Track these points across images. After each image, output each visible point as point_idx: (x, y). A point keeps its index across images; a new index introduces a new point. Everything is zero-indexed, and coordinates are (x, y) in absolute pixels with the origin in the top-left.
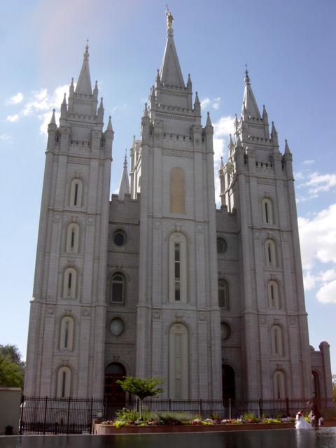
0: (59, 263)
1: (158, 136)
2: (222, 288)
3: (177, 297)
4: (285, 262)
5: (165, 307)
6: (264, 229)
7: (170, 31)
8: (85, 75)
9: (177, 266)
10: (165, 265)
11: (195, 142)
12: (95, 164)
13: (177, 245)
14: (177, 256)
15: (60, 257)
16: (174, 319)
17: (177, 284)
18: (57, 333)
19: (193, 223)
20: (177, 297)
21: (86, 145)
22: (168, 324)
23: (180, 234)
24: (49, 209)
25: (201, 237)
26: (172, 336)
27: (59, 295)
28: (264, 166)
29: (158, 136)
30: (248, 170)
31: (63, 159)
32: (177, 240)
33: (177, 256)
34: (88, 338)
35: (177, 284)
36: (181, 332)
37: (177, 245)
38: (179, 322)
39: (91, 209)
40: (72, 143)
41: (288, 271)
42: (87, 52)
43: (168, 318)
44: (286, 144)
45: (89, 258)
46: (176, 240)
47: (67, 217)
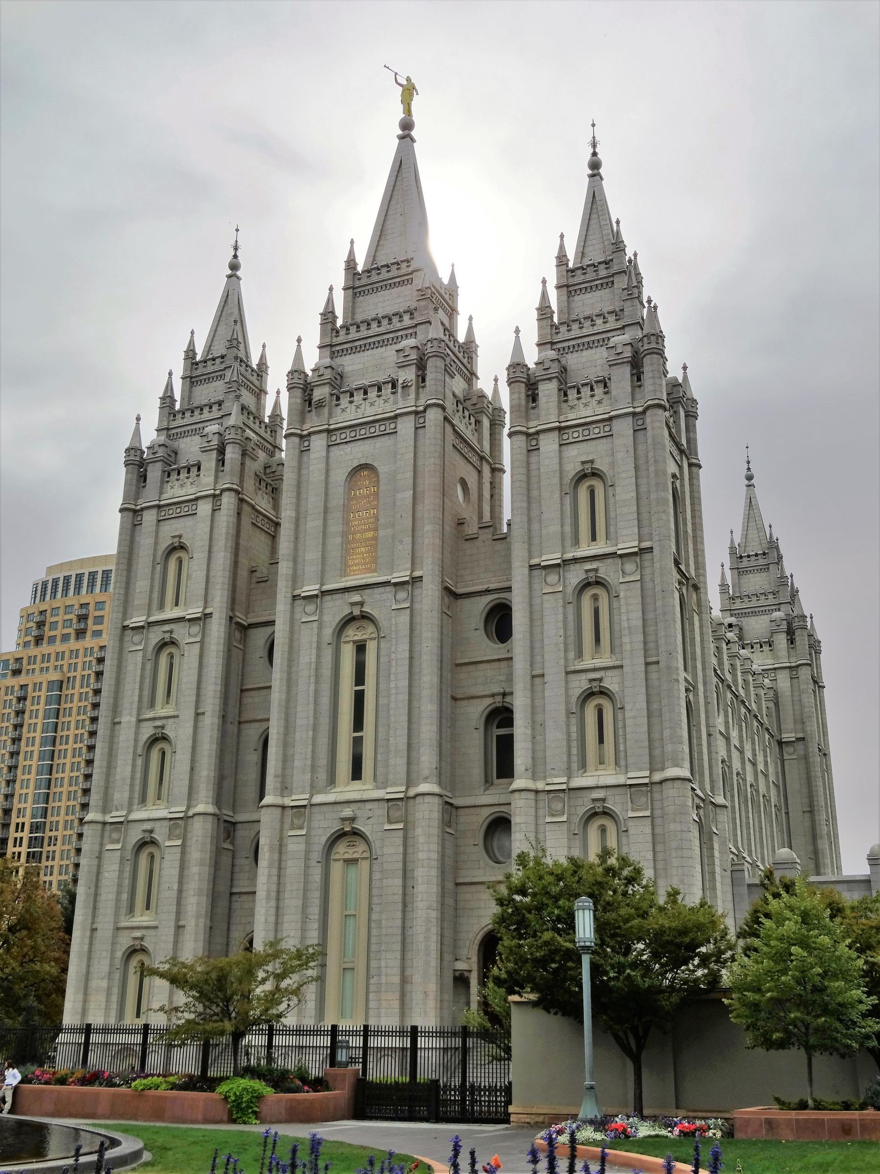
0: (137, 734)
1: (320, 405)
2: (503, 731)
3: (357, 773)
4: (626, 640)
5: (318, 799)
6: (575, 560)
7: (407, 126)
8: (230, 312)
9: (359, 698)
10: (325, 700)
11: (400, 390)
12: (204, 508)
13: (361, 648)
14: (360, 678)
15: (140, 721)
16: (336, 827)
17: (358, 742)
18: (126, 882)
19: (388, 589)
20: (357, 773)
21: (194, 470)
22: (324, 839)
23: (365, 623)
24: (125, 628)
25: (405, 618)
26: (337, 868)
27: (136, 801)
28: (585, 391)
29: (320, 405)
30: (538, 417)
31: (150, 517)
32: (359, 636)
33: (360, 678)
34: (176, 887)
35: (358, 742)
36: (356, 856)
37: (361, 648)
38: (348, 834)
39: (195, 611)
40: (169, 476)
41: (635, 664)
42: (235, 256)
43: (325, 826)
44: (517, 338)
45: (187, 715)
46: (356, 638)
47: (156, 636)
